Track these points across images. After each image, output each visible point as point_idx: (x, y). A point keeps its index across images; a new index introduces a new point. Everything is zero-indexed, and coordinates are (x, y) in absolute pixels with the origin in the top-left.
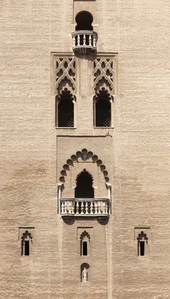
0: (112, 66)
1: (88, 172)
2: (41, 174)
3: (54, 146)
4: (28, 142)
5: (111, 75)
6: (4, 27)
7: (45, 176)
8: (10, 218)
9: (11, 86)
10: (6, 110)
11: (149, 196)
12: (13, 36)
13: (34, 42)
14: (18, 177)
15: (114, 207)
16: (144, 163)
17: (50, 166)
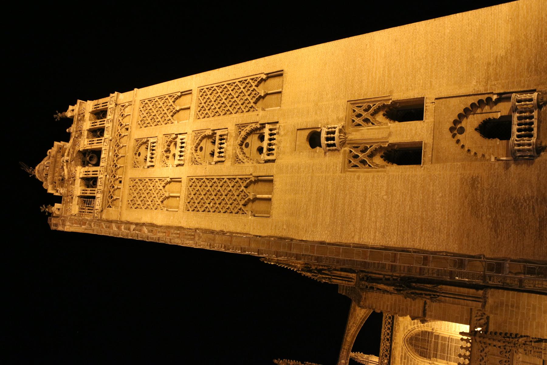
0: (360, 107)
1: (479, 125)
2: (479, 183)
3: (443, 168)
4: (438, 199)
5: (369, 107)
6: (314, 225)
7: (481, 178)
8: (538, 225)
9: (373, 220)
10: (398, 225)
11: (512, 44)
12: (322, 215)
13: (330, 192)
14: (481, 213)
15: (526, 86)
16: (469, 57)
17: (468, 172)
